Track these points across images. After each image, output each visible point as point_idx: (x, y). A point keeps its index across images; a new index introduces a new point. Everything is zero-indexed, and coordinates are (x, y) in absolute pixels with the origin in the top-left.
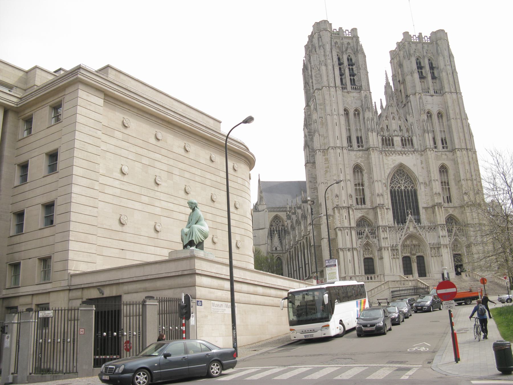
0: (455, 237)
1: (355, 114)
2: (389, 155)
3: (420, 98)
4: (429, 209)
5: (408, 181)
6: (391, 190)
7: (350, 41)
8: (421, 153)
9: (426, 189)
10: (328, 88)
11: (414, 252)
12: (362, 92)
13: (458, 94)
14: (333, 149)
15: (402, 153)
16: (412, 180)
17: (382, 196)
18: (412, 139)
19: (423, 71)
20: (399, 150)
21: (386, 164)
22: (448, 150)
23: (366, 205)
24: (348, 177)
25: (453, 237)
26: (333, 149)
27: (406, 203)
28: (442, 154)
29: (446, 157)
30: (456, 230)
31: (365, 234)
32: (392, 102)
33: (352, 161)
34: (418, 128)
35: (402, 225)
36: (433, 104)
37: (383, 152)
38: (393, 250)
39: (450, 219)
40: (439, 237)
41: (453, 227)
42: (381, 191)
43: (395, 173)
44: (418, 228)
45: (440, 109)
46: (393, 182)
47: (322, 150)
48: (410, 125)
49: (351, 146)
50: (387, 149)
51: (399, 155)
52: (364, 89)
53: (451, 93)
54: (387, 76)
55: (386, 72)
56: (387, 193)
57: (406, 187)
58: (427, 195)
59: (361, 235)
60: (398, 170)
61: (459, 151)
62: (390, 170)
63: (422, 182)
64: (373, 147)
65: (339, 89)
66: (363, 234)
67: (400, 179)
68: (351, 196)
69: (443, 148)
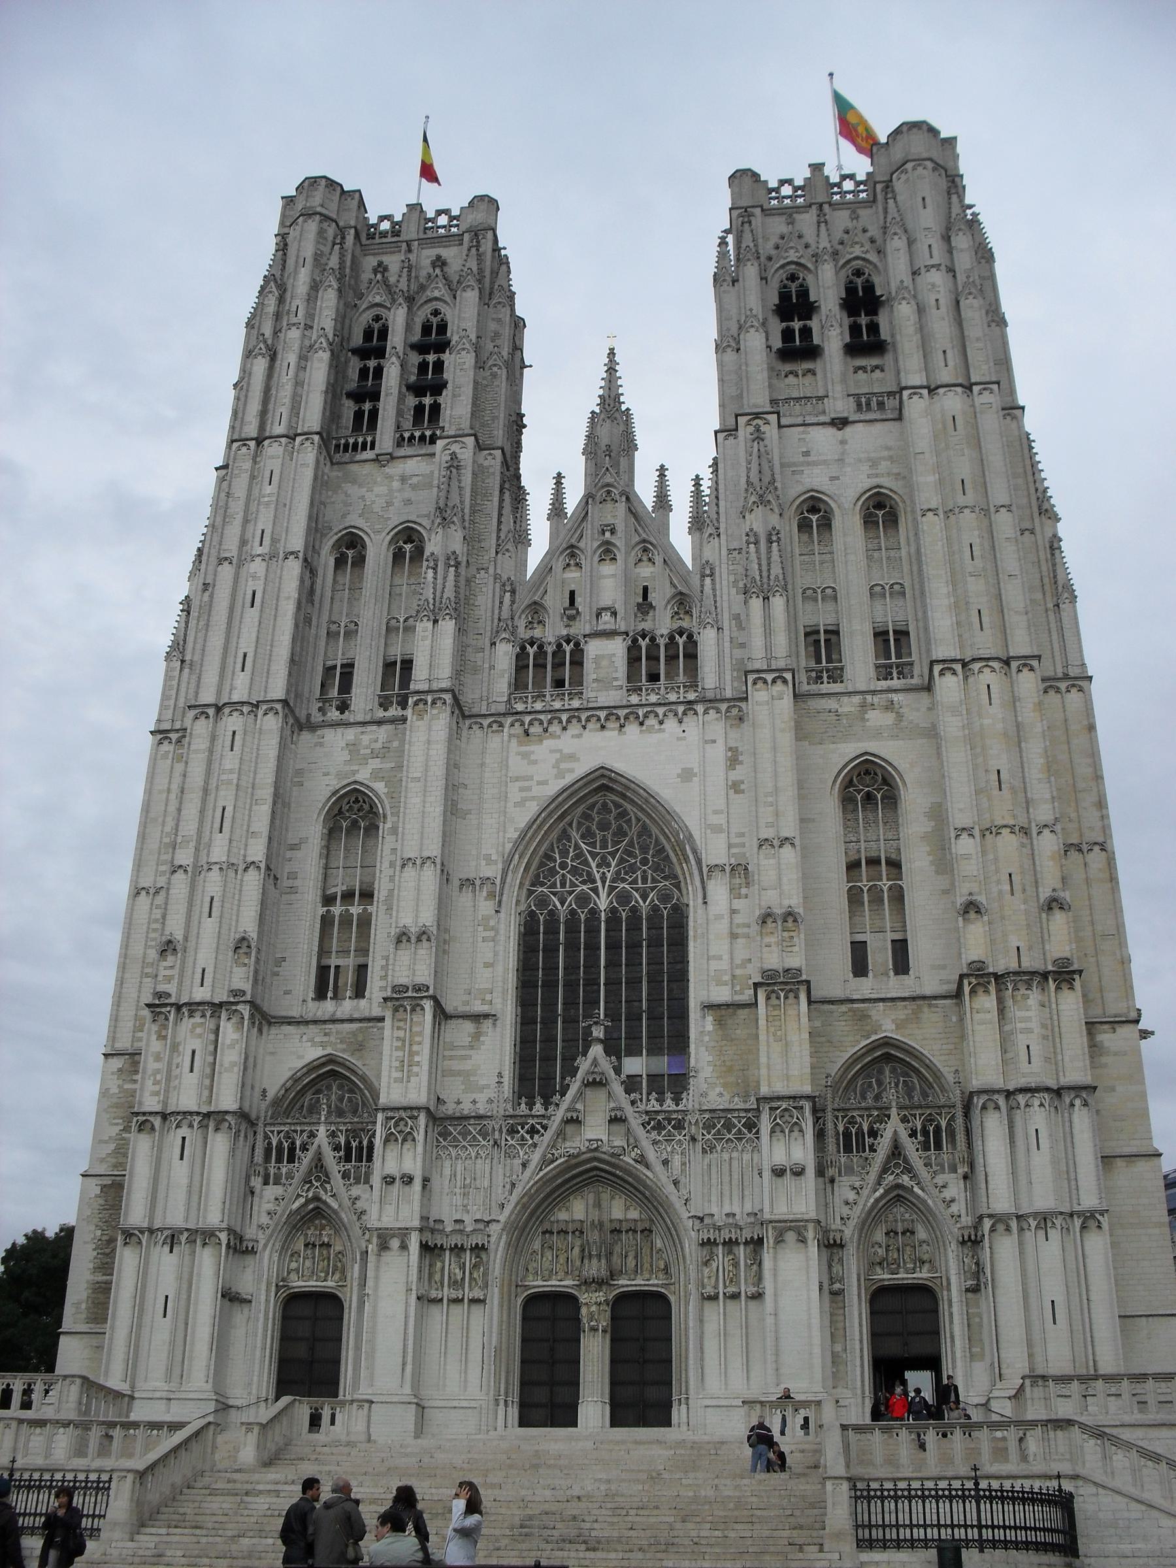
0: (890, 1179)
1: (398, 556)
2: (546, 730)
3: (758, 437)
4: (743, 1013)
5: (644, 862)
6: (532, 914)
7: (447, 253)
8: (735, 711)
9: (738, 904)
10: (252, 444)
11: (595, 1269)
12: (440, 443)
13: (976, 389)
14: (207, 717)
15: (618, 718)
17: (429, 940)
18: (696, 643)
19: (814, 324)
20: (606, 705)
21: (517, 779)
22: (915, 681)
23: (363, 1003)
24: (257, 851)
25: (872, 1177)
26: (207, 717)
27: (612, 983)
28: (863, 706)
29: (889, 718)
30: (904, 1135)
31: (306, 1159)
32: (608, 479)
33: (327, 774)
34: (736, 582)
35: (538, 1108)
36: (841, 460)
37: (510, 720)
38: (458, 1250)
39: (893, 1070)
40: (760, 1174)
41: (884, 1117)
42: (428, 917)
44: (635, 1122)
45: (885, 481)
46: (553, 872)
47: (177, 731)
48: (695, 580)
49: (343, 707)
50: (538, 706)
51: (603, 727)
52: (452, 433)
53: (932, 390)
54: (611, 369)
55: (612, 353)
56: (497, 932)
57: (624, 898)
58: (747, 936)
59: (291, 1160)
61: (955, 673)
62: (533, 808)
63: (722, 860)
64: (424, 687)
65: (308, 444)
67: (594, 857)
68: (241, 944)
69: (884, 672)
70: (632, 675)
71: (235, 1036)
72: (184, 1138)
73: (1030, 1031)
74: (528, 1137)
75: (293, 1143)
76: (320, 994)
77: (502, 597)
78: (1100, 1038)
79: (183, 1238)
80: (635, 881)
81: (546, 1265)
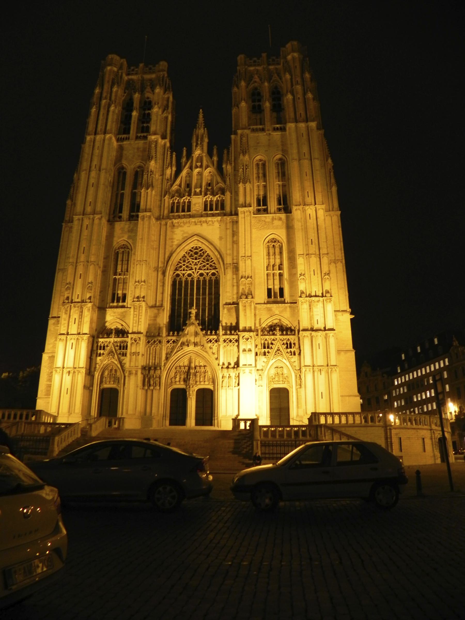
6: (175, 279)
16: (214, 263)
23: (125, 304)
27: (198, 299)
28: (273, 219)
29: (280, 223)
43: (186, 253)
46: (181, 267)
49: (120, 217)
51: (196, 224)
57: (201, 275)
59: (104, 349)
60: (192, 248)
66: (106, 348)
69: (279, 210)
70: (205, 209)
71: (88, 313)
72: (72, 343)
73: (318, 315)
74: (172, 343)
75: (104, 345)
76: (113, 302)
77: (167, 185)
78: (338, 317)
79: (72, 372)
80: (205, 270)
81: (177, 379)
